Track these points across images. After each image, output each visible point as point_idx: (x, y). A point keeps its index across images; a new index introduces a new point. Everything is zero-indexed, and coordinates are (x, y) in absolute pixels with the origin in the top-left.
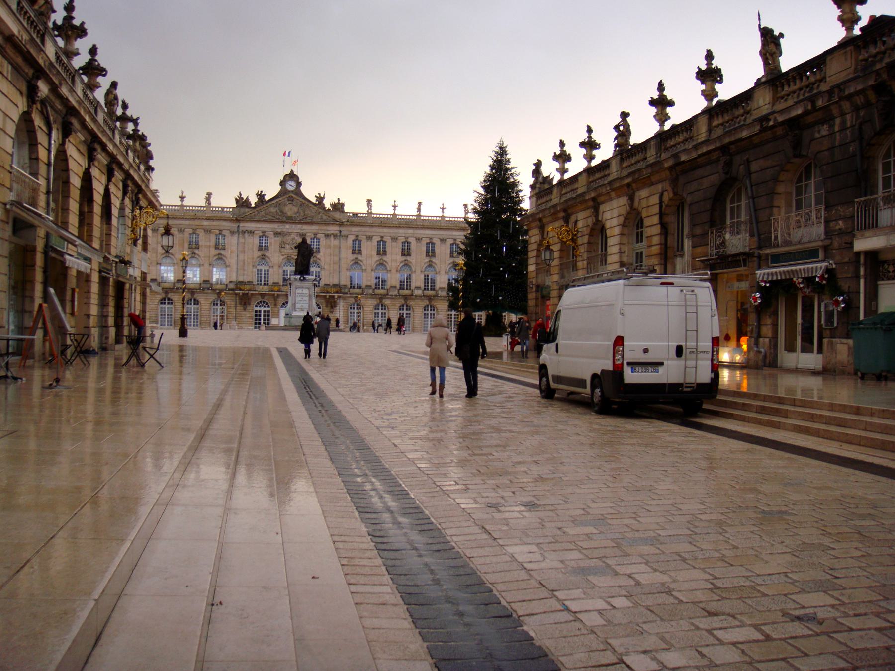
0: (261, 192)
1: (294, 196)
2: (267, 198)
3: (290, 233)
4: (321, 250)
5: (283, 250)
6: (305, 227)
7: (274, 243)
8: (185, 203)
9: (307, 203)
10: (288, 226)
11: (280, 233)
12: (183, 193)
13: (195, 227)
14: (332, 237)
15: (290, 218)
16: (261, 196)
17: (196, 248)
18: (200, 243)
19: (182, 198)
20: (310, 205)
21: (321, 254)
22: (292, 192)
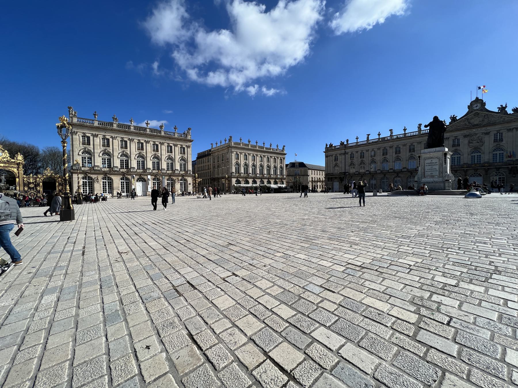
0: (454, 115)
1: (479, 112)
2: (458, 118)
3: (476, 134)
4: (504, 140)
5: (471, 144)
6: (489, 128)
7: (464, 142)
8: (406, 132)
9: (490, 113)
10: (474, 130)
11: (468, 135)
12: (405, 127)
13: (411, 142)
14: (515, 130)
15: (477, 125)
16: (453, 119)
17: (413, 152)
18: (415, 149)
19: (405, 130)
20: (494, 114)
21: (504, 142)
22: (477, 110)
